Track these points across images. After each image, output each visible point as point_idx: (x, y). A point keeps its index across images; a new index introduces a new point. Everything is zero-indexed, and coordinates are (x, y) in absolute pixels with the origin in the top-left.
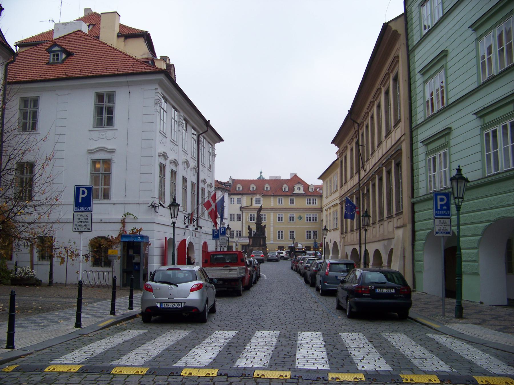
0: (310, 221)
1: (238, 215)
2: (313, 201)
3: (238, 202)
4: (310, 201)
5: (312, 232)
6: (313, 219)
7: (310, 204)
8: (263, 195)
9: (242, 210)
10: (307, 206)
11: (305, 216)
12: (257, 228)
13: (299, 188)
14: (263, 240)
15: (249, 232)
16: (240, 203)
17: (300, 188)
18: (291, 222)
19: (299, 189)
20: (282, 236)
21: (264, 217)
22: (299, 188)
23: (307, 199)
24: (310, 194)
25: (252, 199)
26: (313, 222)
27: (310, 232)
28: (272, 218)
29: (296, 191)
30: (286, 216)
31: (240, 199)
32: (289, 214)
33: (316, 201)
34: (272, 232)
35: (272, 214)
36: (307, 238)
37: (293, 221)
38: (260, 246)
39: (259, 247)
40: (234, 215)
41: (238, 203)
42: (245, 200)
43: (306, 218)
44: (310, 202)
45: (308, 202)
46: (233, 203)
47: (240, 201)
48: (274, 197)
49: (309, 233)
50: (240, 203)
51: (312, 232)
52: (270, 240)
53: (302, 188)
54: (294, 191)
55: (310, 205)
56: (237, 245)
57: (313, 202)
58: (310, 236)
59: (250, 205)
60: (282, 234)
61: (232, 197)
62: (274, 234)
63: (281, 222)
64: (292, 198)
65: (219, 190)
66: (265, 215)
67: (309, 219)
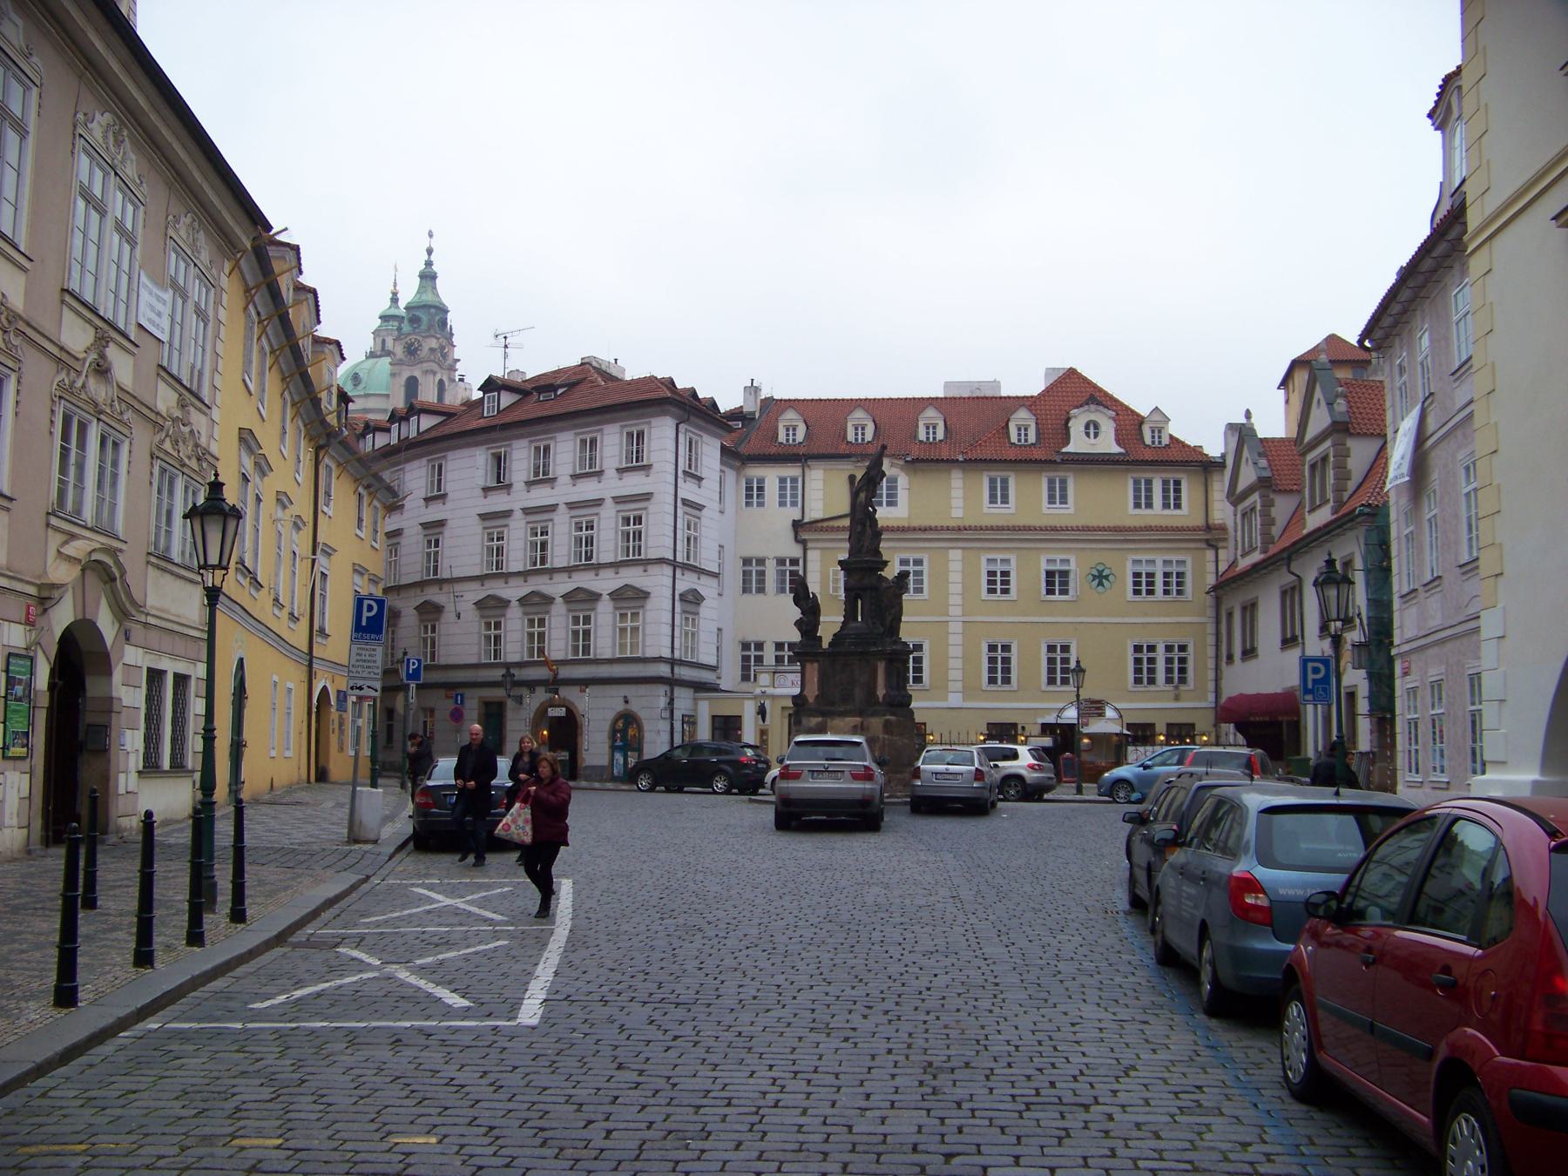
0: (1150, 592)
1: (781, 562)
2: (1165, 490)
3: (783, 496)
4: (1149, 490)
5: (1161, 649)
6: (1166, 584)
7: (1149, 505)
8: (915, 461)
9: (805, 536)
10: (1133, 516)
11: (1125, 566)
12: (852, 593)
13: (1092, 428)
14: (888, 675)
15: (798, 624)
16: (794, 504)
17: (1096, 426)
18: (1051, 597)
19: (1092, 431)
20: (1007, 670)
21: (916, 573)
22: (1092, 428)
23: (1137, 482)
24: (1148, 456)
26: (1168, 598)
27: (1151, 648)
28: (955, 577)
29: (1078, 443)
30: (1027, 569)
31: (794, 480)
33: (1177, 491)
34: (955, 651)
35: (955, 555)
36: (1138, 681)
37: (1064, 592)
38: (869, 706)
39: (861, 714)
40: (761, 561)
41: (782, 504)
42: (820, 485)
43: (1130, 580)
44: (1149, 498)
45: (1137, 497)
46: (761, 504)
47: (792, 493)
48: (964, 471)
49: (1145, 656)
50: (794, 504)
51: (1161, 649)
52: (942, 687)
53: (1108, 428)
54: (1068, 443)
55: (1149, 511)
56: (762, 712)
57: (1165, 497)
58: (1152, 671)
60: (1006, 661)
61: (756, 471)
62: (965, 658)
63: (1005, 597)
64: (1057, 475)
65: (664, 414)
66: (918, 562)
67: (1143, 584)
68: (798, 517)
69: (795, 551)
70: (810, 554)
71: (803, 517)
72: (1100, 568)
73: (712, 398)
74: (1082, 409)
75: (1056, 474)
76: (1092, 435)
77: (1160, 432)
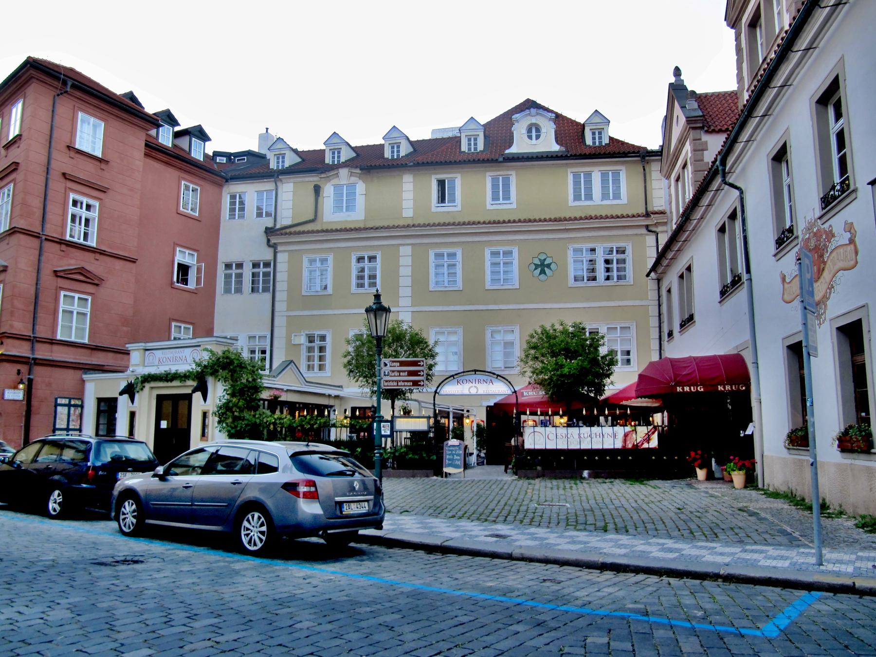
4: (589, 182)
9: (273, 240)
17: (538, 130)
19: (534, 134)
22: (534, 130)
25: (317, 190)
29: (521, 145)
32: (487, 253)
42: (290, 196)
46: (242, 217)
55: (588, 203)
59: (311, 217)
68: (270, 225)
69: (268, 255)
70: (279, 256)
71: (275, 225)
72: (542, 257)
73: (200, 125)
74: (523, 114)
75: (499, 173)
76: (534, 137)
77: (600, 133)
